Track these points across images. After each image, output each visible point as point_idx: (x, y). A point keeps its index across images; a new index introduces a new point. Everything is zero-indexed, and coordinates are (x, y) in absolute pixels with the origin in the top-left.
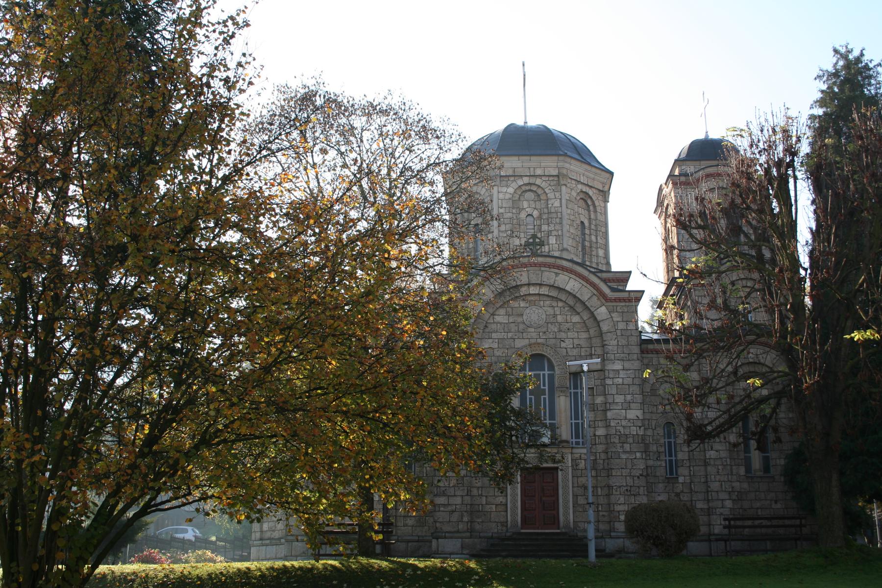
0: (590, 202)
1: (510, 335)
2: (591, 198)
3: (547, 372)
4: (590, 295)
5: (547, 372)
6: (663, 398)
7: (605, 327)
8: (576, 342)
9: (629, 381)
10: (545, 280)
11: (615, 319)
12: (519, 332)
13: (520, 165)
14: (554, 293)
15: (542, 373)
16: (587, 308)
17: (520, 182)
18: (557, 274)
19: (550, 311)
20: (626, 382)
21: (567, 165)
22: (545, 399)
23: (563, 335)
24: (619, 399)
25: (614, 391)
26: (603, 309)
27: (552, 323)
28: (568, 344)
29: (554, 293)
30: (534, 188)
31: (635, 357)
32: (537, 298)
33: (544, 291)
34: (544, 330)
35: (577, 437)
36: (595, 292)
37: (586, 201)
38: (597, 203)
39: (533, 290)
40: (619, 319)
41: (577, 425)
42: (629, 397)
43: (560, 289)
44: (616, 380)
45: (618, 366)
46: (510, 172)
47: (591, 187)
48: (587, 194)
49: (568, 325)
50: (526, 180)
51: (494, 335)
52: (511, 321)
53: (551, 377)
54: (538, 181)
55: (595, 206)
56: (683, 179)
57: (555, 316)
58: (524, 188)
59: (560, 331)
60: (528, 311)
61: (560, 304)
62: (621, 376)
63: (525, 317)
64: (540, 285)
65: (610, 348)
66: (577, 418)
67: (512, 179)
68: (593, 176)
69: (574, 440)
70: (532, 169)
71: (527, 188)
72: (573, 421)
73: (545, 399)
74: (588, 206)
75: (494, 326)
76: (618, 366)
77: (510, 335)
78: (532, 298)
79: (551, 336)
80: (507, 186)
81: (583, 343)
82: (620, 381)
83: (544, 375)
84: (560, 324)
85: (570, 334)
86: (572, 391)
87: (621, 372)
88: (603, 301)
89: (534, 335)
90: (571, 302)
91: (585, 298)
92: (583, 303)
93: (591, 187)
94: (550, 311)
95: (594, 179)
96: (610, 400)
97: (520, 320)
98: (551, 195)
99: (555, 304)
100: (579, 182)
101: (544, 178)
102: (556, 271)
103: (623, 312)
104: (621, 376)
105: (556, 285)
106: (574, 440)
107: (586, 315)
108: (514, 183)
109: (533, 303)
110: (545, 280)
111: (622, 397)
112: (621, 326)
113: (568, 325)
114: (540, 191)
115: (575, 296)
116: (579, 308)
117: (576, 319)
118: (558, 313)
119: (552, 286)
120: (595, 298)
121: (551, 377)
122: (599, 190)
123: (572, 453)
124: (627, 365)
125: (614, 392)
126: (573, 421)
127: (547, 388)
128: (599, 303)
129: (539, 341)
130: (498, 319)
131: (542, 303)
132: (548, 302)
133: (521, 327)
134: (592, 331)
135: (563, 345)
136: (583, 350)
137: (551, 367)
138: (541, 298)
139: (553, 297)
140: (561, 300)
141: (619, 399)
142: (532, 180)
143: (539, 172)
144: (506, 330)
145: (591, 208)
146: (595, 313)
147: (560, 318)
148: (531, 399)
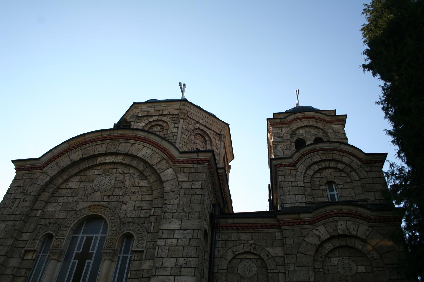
0: (207, 138)
1: (76, 198)
2: (208, 135)
4: (159, 159)
5: (100, 235)
6: (241, 277)
7: (168, 187)
8: (138, 204)
9: (185, 242)
10: (121, 149)
11: (180, 180)
12: (85, 196)
13: (152, 109)
14: (127, 161)
16: (155, 172)
17: (151, 119)
18: (133, 144)
19: (121, 177)
20: (180, 243)
21: (188, 109)
22: (89, 263)
23: (127, 198)
24: (170, 262)
25: (164, 253)
26: (170, 171)
27: (118, 188)
28: (130, 206)
29: (127, 161)
30: (161, 123)
31: (197, 215)
32: (112, 166)
33: (119, 159)
34: (109, 194)
36: (165, 156)
37: (204, 137)
38: (213, 140)
39: (109, 159)
40: (185, 179)
42: (181, 261)
43: (134, 157)
44: (169, 241)
45: (175, 225)
46: (145, 114)
47: (209, 129)
48: (205, 132)
49: (133, 189)
50: (155, 118)
51: (61, 199)
52: (81, 186)
54: (164, 118)
55: (211, 142)
56: (278, 121)
57: (124, 181)
58: (153, 124)
59: (125, 194)
60: (100, 178)
61: (132, 171)
62: (176, 236)
63: (95, 183)
64: (116, 154)
65: (170, 206)
67: (146, 118)
68: (211, 122)
70: (161, 112)
71: (156, 123)
73: (89, 263)
74: (206, 141)
75: (64, 192)
76: (175, 225)
77: (76, 198)
78: (107, 167)
79: (114, 199)
80: (141, 122)
81: (145, 205)
82: (174, 241)
83: (97, 237)
84: (127, 188)
85: (134, 197)
86: (122, 255)
87: (177, 232)
88: (171, 163)
89: (98, 199)
90: (141, 167)
91: (154, 162)
92: (151, 166)
93: (209, 129)
94: (121, 177)
95: (212, 124)
96: (158, 265)
97: (89, 185)
98: (172, 126)
99: (126, 171)
100: (198, 122)
101: (168, 116)
102: (133, 141)
103: (189, 173)
104: (176, 236)
105: (130, 153)
107: (152, 179)
108: (147, 120)
109: (106, 171)
110: (121, 150)
111: (173, 261)
112: (186, 185)
113: (133, 189)
114: (164, 125)
115: (146, 163)
116: (148, 173)
117: (144, 183)
118: (127, 178)
119: (126, 155)
120: (164, 162)
121: (103, 239)
122: (217, 133)
124: (185, 224)
125: (164, 254)
127: (95, 252)
128: (167, 166)
129: (102, 203)
130: (70, 185)
131: (114, 171)
132: (120, 170)
133: (89, 191)
134: (155, 193)
135: (124, 207)
136: (143, 212)
138: (116, 166)
140: (133, 167)
141: (170, 262)
142: (160, 118)
143: (165, 113)
144: (74, 194)
145: (208, 142)
146: (161, 174)
147: (127, 183)
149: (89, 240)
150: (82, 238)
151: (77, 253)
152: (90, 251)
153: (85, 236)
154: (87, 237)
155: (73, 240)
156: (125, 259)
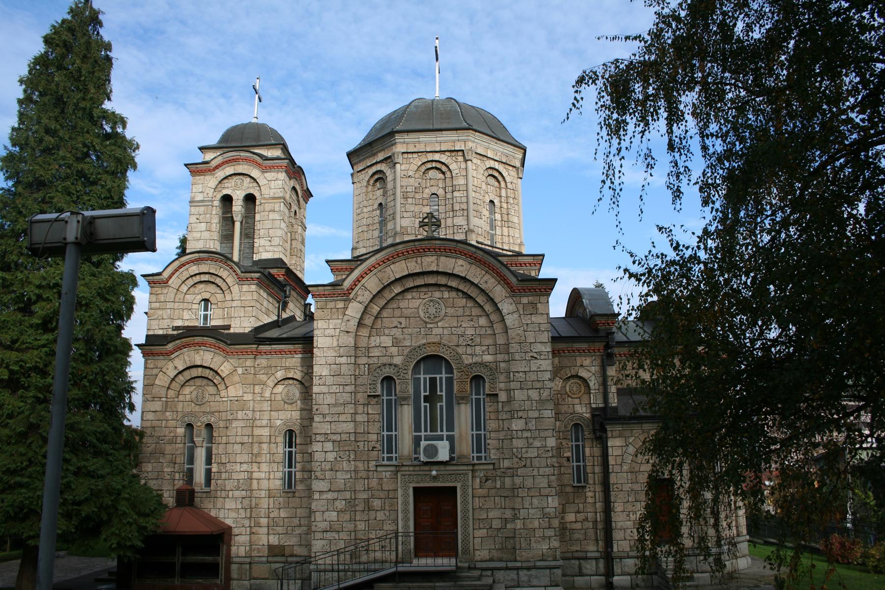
3: (444, 376)
5: (444, 376)
15: (438, 376)
22: (441, 407)
35: (479, 451)
41: (479, 437)
53: (450, 381)
66: (478, 428)
69: (475, 455)
72: (475, 432)
73: (441, 407)
83: (441, 379)
106: (475, 455)
123: (472, 470)
126: (475, 432)
127: (444, 394)
137: (450, 370)
139: (451, 287)
148: (425, 407)
149: (433, 381)
150: (425, 379)
151: (425, 396)
152: (439, 393)
153: (428, 377)
154: (430, 378)
155: (417, 381)
156: (478, 401)
